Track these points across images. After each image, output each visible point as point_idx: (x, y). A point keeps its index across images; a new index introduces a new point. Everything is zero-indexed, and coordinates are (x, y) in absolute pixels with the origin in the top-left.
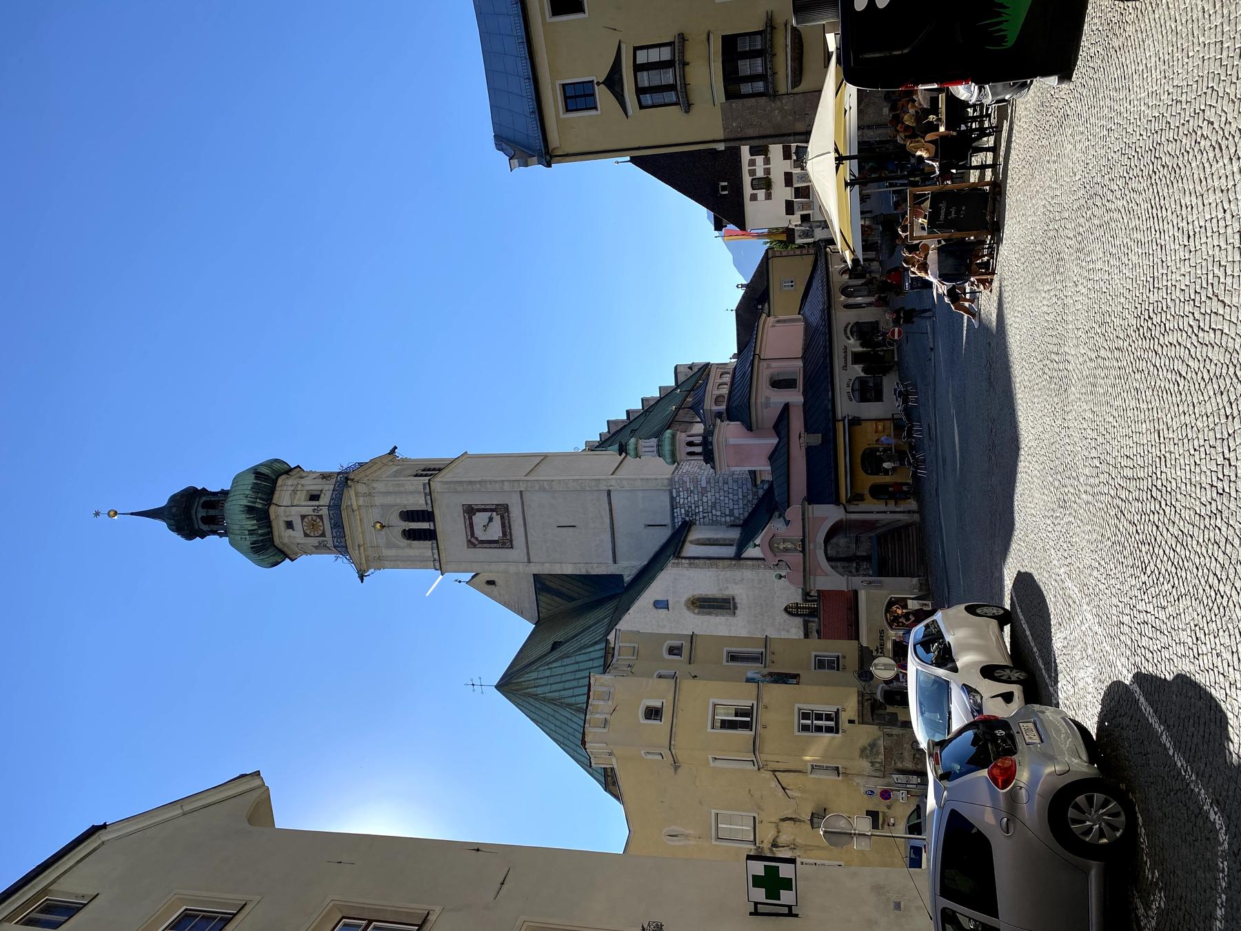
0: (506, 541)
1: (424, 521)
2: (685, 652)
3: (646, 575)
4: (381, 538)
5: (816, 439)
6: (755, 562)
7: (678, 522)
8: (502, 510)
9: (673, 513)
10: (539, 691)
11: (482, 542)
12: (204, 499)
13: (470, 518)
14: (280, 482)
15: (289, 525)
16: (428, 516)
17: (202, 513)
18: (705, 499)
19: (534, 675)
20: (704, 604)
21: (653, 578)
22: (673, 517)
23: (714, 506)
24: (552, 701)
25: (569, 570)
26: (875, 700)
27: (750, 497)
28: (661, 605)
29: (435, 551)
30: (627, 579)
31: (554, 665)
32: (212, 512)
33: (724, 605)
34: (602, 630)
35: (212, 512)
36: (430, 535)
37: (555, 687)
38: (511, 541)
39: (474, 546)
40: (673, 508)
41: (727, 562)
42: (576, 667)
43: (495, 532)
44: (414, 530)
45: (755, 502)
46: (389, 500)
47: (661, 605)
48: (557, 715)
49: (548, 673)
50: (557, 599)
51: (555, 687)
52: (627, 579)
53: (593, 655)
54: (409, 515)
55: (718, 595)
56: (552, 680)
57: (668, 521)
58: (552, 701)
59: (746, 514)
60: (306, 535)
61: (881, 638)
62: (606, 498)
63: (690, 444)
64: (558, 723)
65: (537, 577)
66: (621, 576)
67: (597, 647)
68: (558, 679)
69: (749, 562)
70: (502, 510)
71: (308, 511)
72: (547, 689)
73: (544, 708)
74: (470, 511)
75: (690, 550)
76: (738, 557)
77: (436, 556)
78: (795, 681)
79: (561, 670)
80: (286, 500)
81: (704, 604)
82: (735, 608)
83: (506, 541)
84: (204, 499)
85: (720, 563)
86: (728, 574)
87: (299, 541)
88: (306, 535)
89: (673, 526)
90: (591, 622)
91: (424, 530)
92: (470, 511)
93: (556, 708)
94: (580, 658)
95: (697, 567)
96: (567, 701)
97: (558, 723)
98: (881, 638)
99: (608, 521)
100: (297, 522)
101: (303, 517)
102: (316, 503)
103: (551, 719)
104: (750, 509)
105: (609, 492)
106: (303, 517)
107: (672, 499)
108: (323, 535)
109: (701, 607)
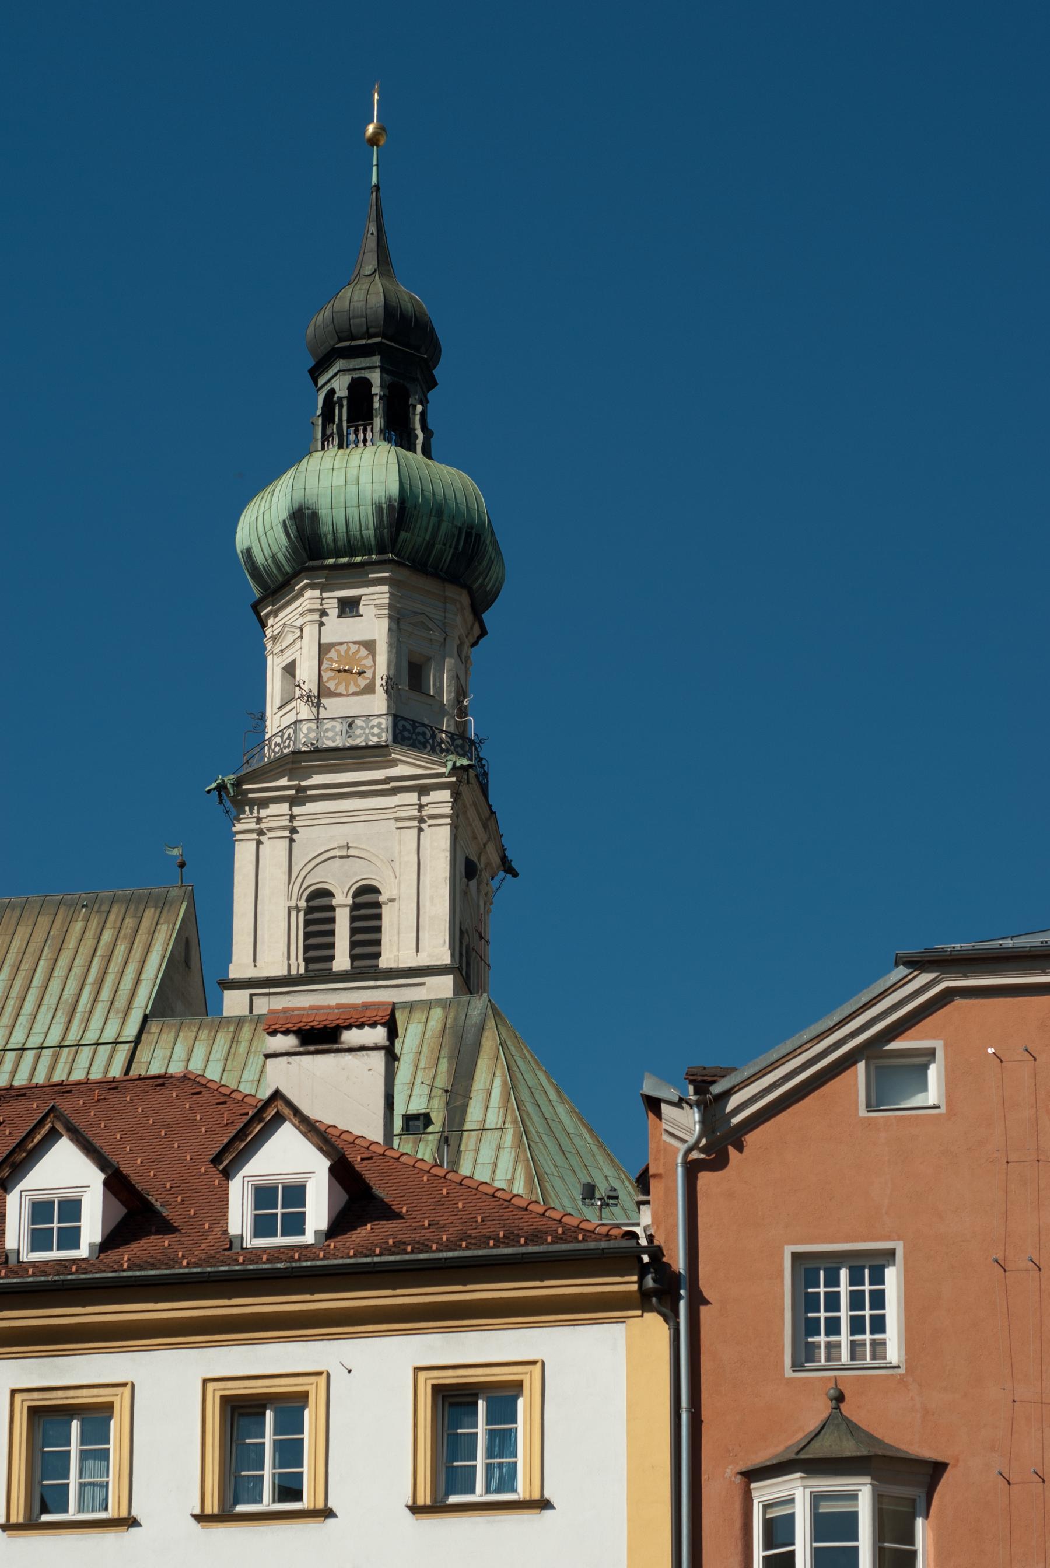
14: (451, 591)
36: (317, 965)
54: (368, 905)
106: (370, 645)
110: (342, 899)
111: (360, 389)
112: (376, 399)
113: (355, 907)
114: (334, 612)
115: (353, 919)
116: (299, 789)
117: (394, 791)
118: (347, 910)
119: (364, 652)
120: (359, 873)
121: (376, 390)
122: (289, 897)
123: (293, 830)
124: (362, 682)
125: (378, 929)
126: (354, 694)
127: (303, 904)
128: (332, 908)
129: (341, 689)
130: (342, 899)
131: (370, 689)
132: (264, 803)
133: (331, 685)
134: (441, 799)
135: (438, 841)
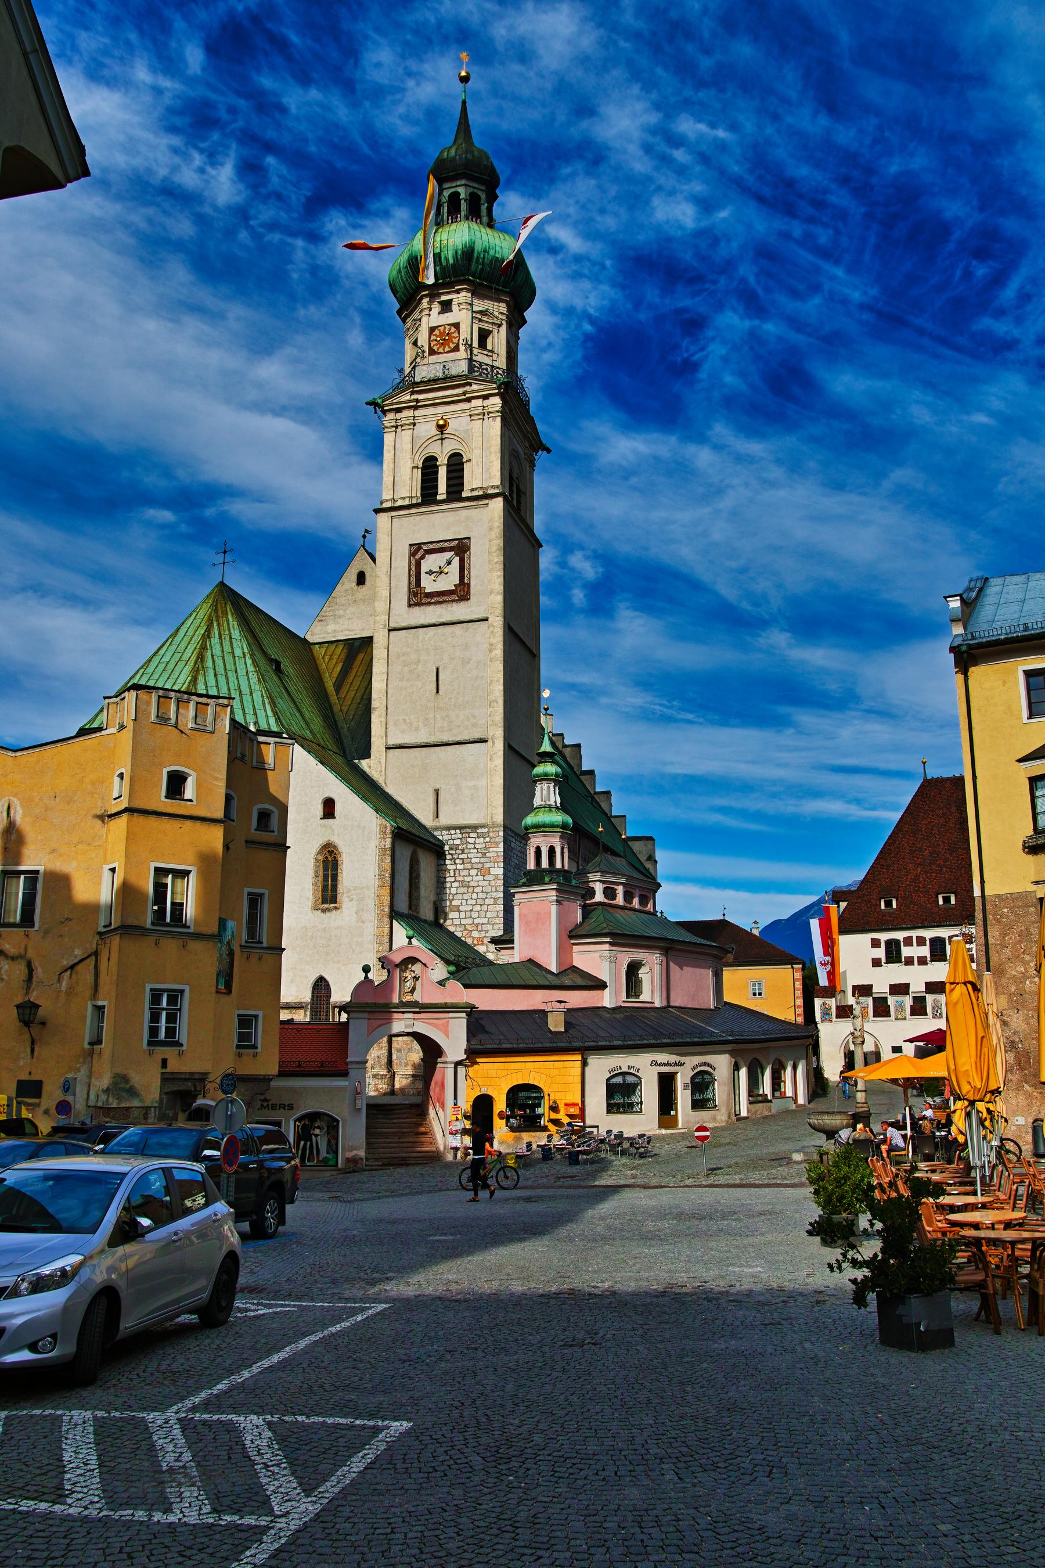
0: (418, 597)
1: (448, 486)
2: (263, 836)
3: (371, 791)
4: (427, 429)
5: (556, 1024)
6: (386, 939)
7: (443, 836)
8: (462, 592)
9: (455, 828)
10: (215, 640)
11: (418, 565)
12: (483, 196)
13: (451, 549)
15: (446, 307)
16: (455, 492)
17: (463, 192)
18: (473, 872)
19: (236, 633)
20: (329, 862)
21: (365, 798)
22: (449, 828)
23: (464, 884)
24: (201, 657)
25: (378, 684)
26: (194, 1098)
27: (475, 934)
28: (329, 808)
29: (407, 502)
30: (364, 764)
31: (249, 662)
32: (464, 206)
33: (329, 893)
34: (295, 728)
35: (464, 206)
36: (428, 496)
37: (219, 662)
38: (419, 604)
39: (412, 554)
40: (460, 828)
41: (387, 900)
42: (245, 689)
43: (429, 584)
44: (437, 473)
45: (469, 941)
46: (477, 442)
47: (329, 808)
48: (182, 664)
49: (238, 652)
50: (338, 669)
51: (219, 662)
52: (364, 764)
53: (261, 714)
54: (456, 464)
55: (341, 888)
56: (229, 658)
57: (444, 820)
58: (201, 657)
59: (451, 929)
60: (432, 330)
61: (282, 1106)
62: (476, 736)
63: (552, 851)
64: (171, 666)
65: (370, 639)
66: (367, 755)
67: (272, 721)
68: (230, 666)
69: (387, 931)
70: (462, 592)
71: (464, 333)
72: (217, 650)
73: (191, 647)
74: (461, 548)
75: (405, 853)
76: (394, 914)
77: (399, 503)
78: (222, 987)
79: (241, 671)
80: (480, 305)
81: (329, 862)
82: (324, 911)
83: (418, 597)
84: (483, 196)
85: (386, 891)
86: (371, 903)
87: (425, 319)
88: (432, 330)
89: (437, 829)
90: (307, 715)
91: (436, 487)
92: (461, 548)
93: (191, 663)
94: (257, 696)
95: (381, 858)
96: (201, 678)
97: (171, 666)
98: (282, 1106)
99: (445, 739)
100: (449, 318)
101: (456, 326)
102: (475, 344)
103: (177, 656)
104: (459, 934)
105: (485, 741)
106: (456, 326)
107: (474, 828)
108: (432, 352)
109: (326, 861)
110: (443, 461)
111: (455, 198)
112: (462, 202)
113: (448, 466)
114: (436, 308)
115: (448, 472)
116: (417, 401)
117: (469, 400)
118: (445, 467)
119: (453, 329)
120: (450, 446)
121: (462, 196)
122: (413, 460)
123: (414, 424)
124: (452, 346)
125: (462, 477)
126: (448, 352)
127: (420, 466)
128: (437, 467)
129: (441, 350)
130: (443, 461)
131: (456, 349)
132: (398, 410)
133: (435, 348)
134: (496, 402)
135: (495, 426)
